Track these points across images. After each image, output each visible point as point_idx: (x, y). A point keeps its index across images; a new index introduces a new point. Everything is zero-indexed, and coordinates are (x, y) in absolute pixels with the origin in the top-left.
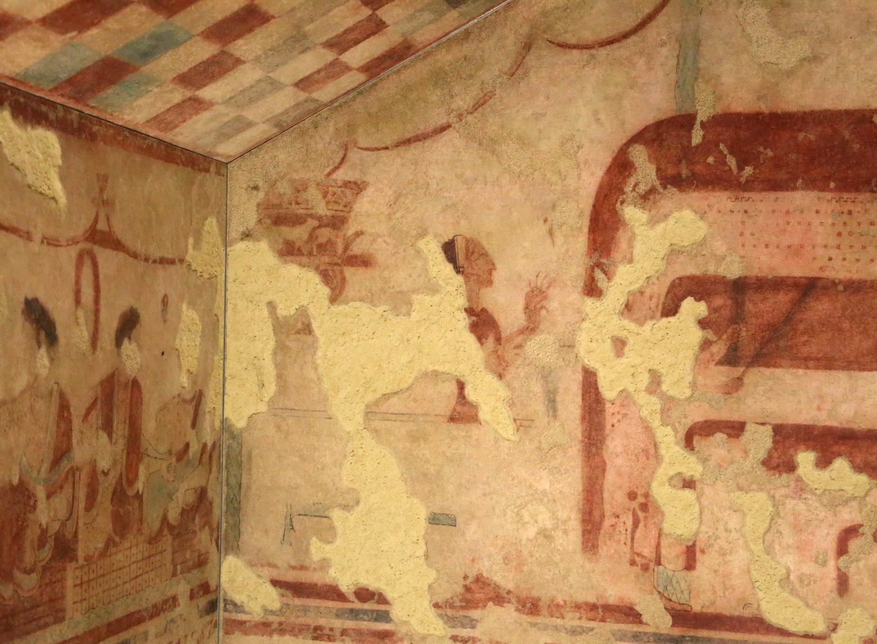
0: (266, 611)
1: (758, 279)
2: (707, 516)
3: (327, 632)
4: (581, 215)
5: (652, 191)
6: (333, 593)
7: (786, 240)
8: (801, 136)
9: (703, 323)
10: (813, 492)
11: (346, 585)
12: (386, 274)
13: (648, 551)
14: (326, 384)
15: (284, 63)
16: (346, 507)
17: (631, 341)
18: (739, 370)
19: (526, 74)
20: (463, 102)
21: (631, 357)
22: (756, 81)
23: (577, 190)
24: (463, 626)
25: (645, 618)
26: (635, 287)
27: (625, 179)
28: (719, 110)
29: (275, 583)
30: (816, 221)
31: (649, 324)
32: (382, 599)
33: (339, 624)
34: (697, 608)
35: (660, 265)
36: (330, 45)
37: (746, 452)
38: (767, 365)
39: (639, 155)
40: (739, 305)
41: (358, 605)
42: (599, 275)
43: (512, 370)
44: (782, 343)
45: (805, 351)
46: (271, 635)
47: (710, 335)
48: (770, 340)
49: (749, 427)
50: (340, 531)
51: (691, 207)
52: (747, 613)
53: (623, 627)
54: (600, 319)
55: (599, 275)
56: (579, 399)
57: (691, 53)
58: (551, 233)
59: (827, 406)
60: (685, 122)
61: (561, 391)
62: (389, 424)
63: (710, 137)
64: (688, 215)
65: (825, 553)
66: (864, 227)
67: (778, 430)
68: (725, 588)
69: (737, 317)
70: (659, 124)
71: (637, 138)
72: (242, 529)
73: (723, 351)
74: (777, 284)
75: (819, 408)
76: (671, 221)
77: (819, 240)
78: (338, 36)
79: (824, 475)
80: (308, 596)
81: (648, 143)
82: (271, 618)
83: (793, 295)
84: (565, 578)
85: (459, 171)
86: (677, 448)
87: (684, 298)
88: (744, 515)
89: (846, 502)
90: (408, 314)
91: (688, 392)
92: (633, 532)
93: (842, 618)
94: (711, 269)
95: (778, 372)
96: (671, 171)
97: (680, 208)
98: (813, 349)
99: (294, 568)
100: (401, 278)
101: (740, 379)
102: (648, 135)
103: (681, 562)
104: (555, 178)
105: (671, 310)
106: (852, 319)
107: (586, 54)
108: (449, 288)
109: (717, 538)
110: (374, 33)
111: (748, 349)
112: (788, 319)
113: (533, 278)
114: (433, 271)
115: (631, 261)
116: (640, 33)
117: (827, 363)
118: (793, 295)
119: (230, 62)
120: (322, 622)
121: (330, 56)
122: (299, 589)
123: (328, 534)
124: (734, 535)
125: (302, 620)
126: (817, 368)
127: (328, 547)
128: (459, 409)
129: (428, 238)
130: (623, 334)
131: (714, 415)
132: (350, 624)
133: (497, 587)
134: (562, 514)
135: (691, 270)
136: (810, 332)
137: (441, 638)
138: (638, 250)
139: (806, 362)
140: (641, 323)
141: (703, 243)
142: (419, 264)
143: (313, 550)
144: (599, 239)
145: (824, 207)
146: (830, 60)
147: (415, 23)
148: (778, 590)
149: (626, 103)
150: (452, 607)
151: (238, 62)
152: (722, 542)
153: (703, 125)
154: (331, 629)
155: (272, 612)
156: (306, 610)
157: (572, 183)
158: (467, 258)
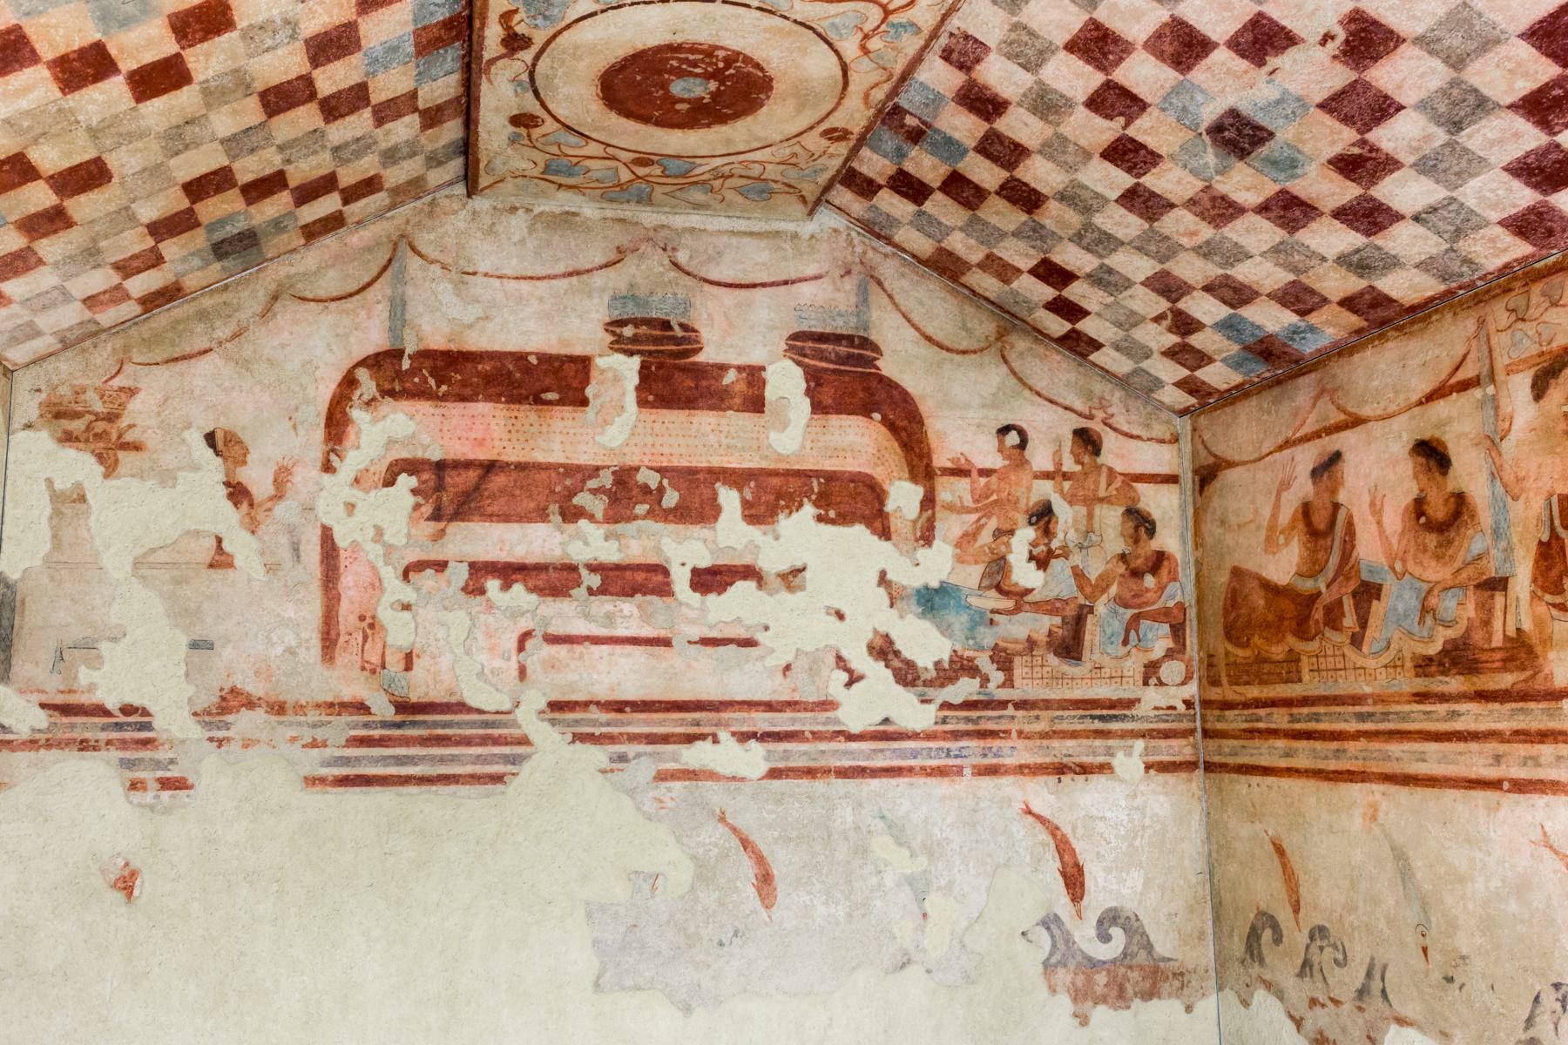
0: (33, 730)
1: (454, 461)
2: (420, 630)
3: (92, 743)
4: (318, 415)
5: (373, 399)
6: (101, 711)
7: (473, 435)
8: (480, 367)
9: (414, 492)
10: (498, 609)
11: (112, 703)
12: (155, 456)
13: (375, 659)
14: (98, 543)
15: (77, 275)
16: (114, 639)
17: (359, 504)
18: (442, 525)
19: (275, 315)
20: (223, 332)
21: (359, 516)
22: (447, 330)
23: (315, 398)
24: (219, 729)
25: (373, 711)
26: (362, 466)
27: (352, 392)
28: (421, 347)
29: (43, 706)
30: (493, 422)
31: (373, 493)
32: (145, 712)
33: (103, 736)
34: (414, 699)
35: (381, 451)
36: (118, 267)
37: (449, 582)
38: (463, 520)
39: (363, 375)
40: (440, 479)
41: (122, 719)
42: (333, 457)
43: (262, 527)
44: (473, 505)
45: (489, 510)
46: (37, 750)
47: (420, 500)
48: (464, 503)
49: (450, 564)
50: (106, 660)
51: (402, 410)
52: (453, 700)
53: (355, 718)
54: (335, 489)
55: (333, 457)
56: (318, 548)
57: (400, 308)
58: (295, 427)
59: (507, 547)
60: (397, 354)
61: (304, 542)
62: (155, 572)
63: (415, 365)
64: (401, 417)
65: (510, 651)
66: (526, 427)
67: (472, 565)
68: (436, 682)
69: (440, 487)
70: (377, 355)
71: (362, 363)
72: (13, 662)
73: (430, 511)
74: (468, 464)
75: (501, 549)
76: (388, 421)
77: (496, 435)
78: (124, 260)
79: (507, 596)
80: (76, 715)
81: (369, 367)
82: (38, 736)
83: (479, 472)
84: (308, 684)
85: (219, 382)
86: (397, 582)
87: (399, 473)
88: (449, 628)
89: (522, 614)
90: (174, 486)
91: (404, 541)
92: (363, 645)
93: (523, 698)
94: (420, 454)
95: (470, 524)
96: (387, 386)
97: (394, 412)
98: (494, 508)
99: (62, 692)
100: (168, 459)
101: (443, 530)
102: (369, 362)
103: (402, 665)
104: (297, 389)
105: (390, 482)
106: (522, 488)
107: (321, 305)
108: (210, 467)
109: (429, 646)
110: (153, 266)
111: (450, 510)
112: (477, 488)
113: (280, 460)
114: (196, 455)
115: (358, 448)
116: (362, 294)
117: (505, 518)
118: (479, 472)
119: (33, 260)
120: (88, 735)
121: (115, 279)
122: (66, 710)
123: (96, 662)
124: (442, 643)
125: (68, 735)
126: (498, 522)
127: (96, 674)
128: (217, 558)
129: (192, 430)
130: (353, 500)
131: (424, 557)
132: (115, 735)
133: (249, 695)
134: (305, 635)
135: (405, 455)
136: (493, 497)
137: (198, 740)
138: (364, 440)
139: (490, 517)
140: (367, 491)
141: (413, 436)
142: (184, 448)
143: (81, 676)
144: (333, 432)
145: (498, 413)
146: (497, 320)
147: (186, 266)
148: (476, 681)
149: (352, 340)
150: (209, 714)
151: (40, 262)
152: (433, 649)
153: (410, 357)
154: (97, 741)
155: (40, 731)
156: (72, 726)
157: (311, 392)
158: (225, 444)
